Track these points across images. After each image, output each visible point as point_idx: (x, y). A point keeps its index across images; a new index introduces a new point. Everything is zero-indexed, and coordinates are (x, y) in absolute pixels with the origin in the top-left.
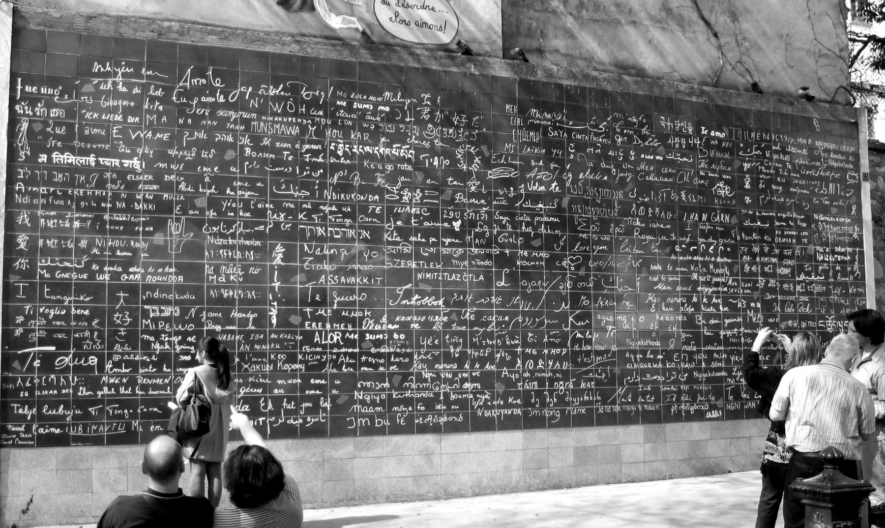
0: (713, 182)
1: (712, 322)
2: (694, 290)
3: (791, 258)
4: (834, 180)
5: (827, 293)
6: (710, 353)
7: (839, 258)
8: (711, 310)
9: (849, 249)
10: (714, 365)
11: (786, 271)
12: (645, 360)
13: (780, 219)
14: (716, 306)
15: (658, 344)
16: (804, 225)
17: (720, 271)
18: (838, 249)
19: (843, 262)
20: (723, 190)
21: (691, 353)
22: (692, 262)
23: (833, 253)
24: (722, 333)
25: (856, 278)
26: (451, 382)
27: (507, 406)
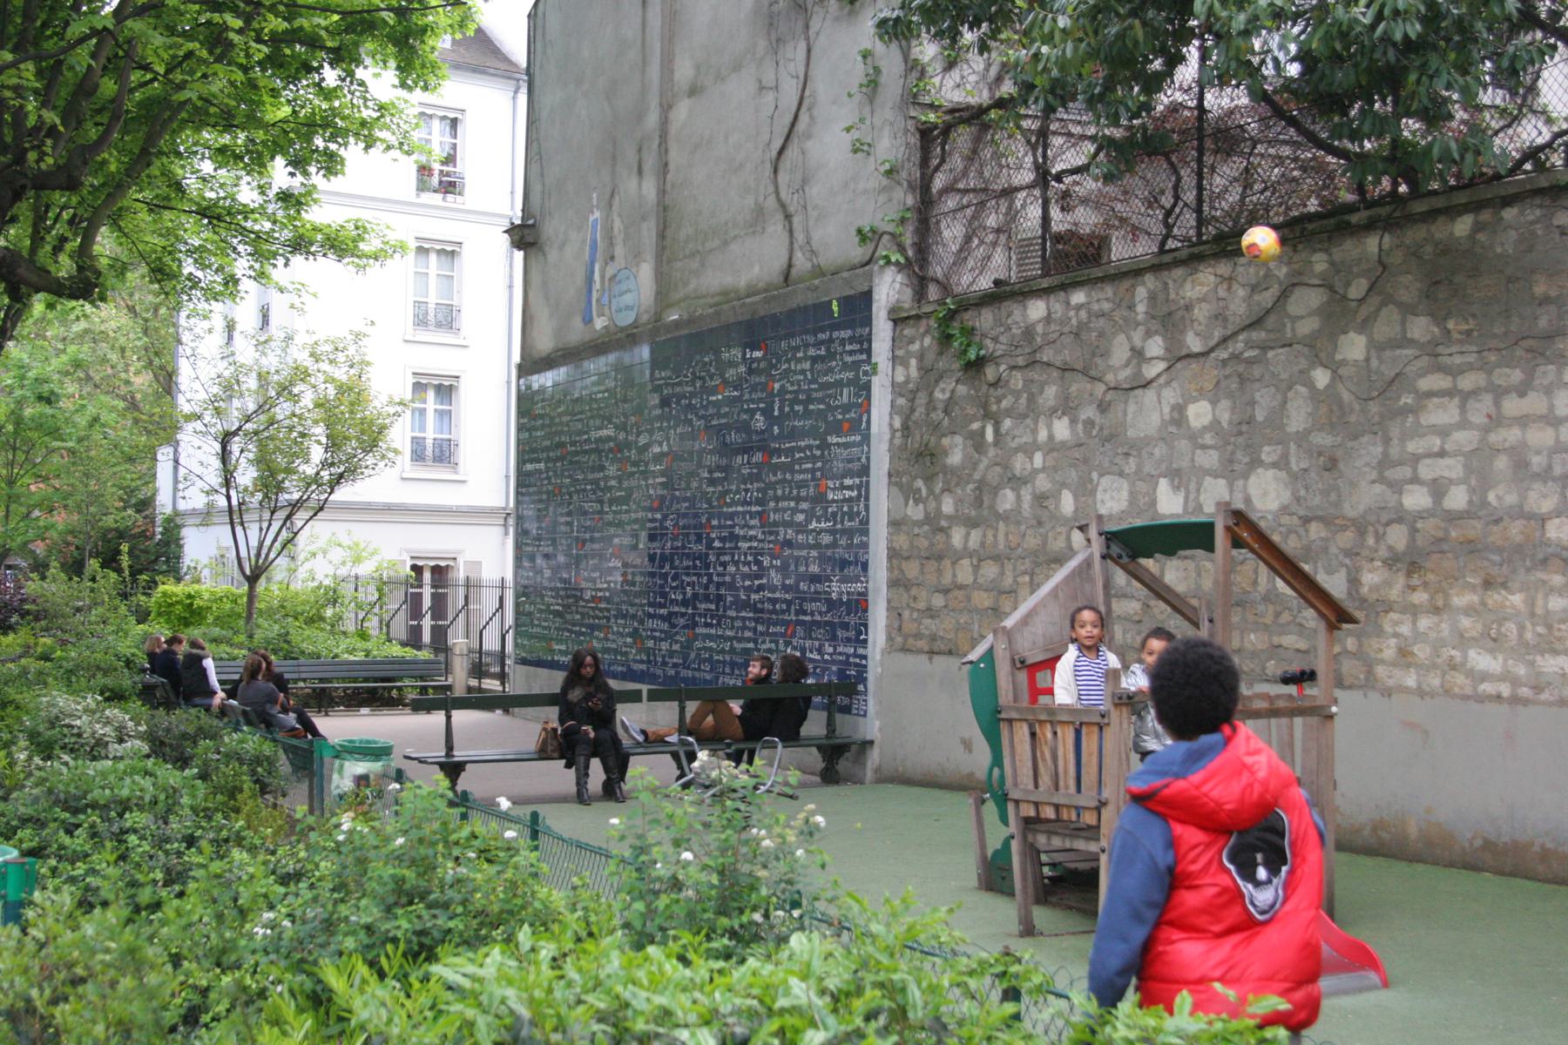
0: (752, 412)
1: (748, 583)
2: (737, 548)
3: (805, 499)
4: (850, 383)
5: (834, 545)
6: (744, 619)
7: (847, 493)
8: (746, 569)
9: (857, 481)
10: (748, 634)
11: (800, 517)
12: (707, 625)
13: (801, 450)
14: (749, 563)
15: (713, 607)
16: (818, 453)
17: (752, 522)
18: (848, 482)
19: (850, 499)
20: (759, 422)
21: (733, 619)
22: (737, 513)
23: (843, 487)
24: (753, 596)
25: (861, 522)
26: (621, 635)
27: (642, 662)
